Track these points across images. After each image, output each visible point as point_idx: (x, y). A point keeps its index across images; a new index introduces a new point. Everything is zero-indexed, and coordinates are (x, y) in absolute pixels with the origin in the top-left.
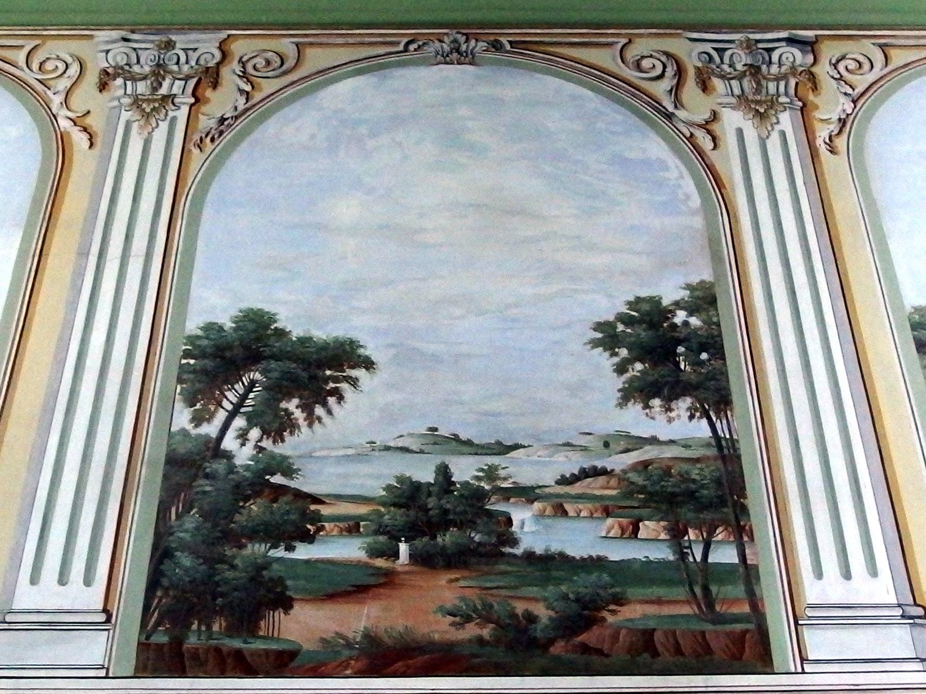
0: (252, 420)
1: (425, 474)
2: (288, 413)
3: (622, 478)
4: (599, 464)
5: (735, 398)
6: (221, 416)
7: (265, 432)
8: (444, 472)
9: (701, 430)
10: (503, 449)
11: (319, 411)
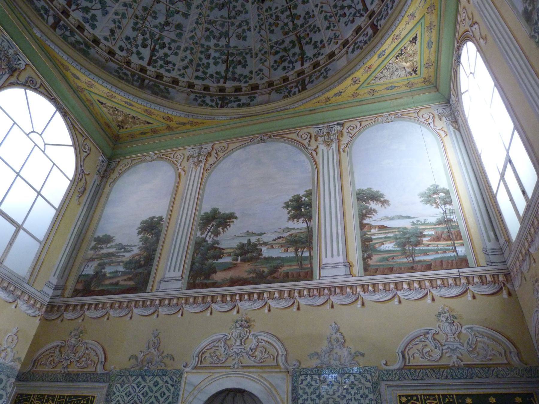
0: (212, 233)
1: (245, 241)
2: (219, 231)
3: (286, 238)
4: (282, 235)
5: (313, 217)
6: (206, 232)
7: (214, 235)
8: (249, 240)
9: (305, 225)
10: (261, 234)
11: (225, 229)
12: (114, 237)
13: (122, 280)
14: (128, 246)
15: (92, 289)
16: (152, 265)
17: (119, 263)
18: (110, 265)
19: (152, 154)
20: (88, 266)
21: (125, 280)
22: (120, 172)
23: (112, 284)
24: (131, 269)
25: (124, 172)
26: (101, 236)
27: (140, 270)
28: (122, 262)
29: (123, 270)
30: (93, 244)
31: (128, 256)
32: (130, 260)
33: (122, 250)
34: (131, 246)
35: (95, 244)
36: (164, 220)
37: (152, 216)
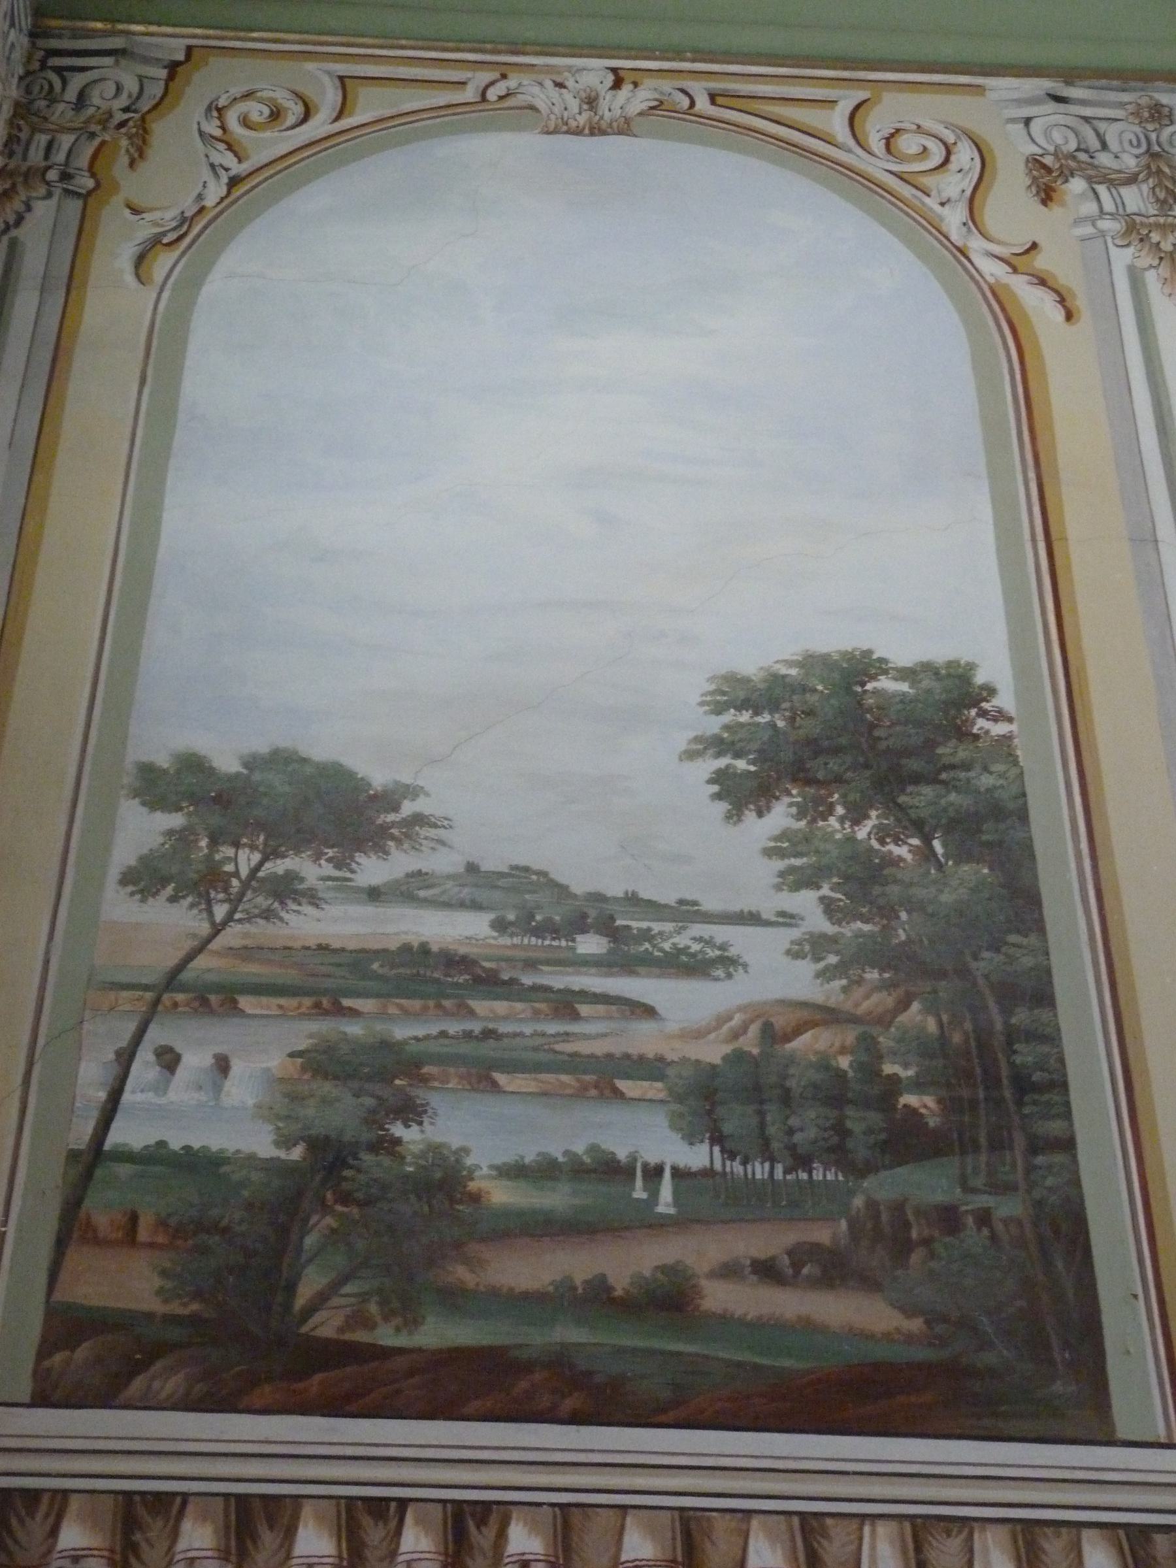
12: (413, 792)
13: (728, 1271)
14: (632, 899)
15: (326, 1325)
16: (1068, 1145)
17: (604, 1079)
18: (482, 1077)
19: (593, 72)
20: (169, 1060)
21: (766, 1271)
22: (229, 160)
23: (597, 1299)
24: (802, 1161)
25: (293, 170)
26: (227, 763)
27: (927, 1184)
28: (649, 1068)
29: (698, 1156)
30: (141, 830)
31: (688, 1015)
32: (738, 1058)
33: (590, 945)
34: (686, 912)
35: (182, 838)
36: (1005, 700)
37: (837, 639)
